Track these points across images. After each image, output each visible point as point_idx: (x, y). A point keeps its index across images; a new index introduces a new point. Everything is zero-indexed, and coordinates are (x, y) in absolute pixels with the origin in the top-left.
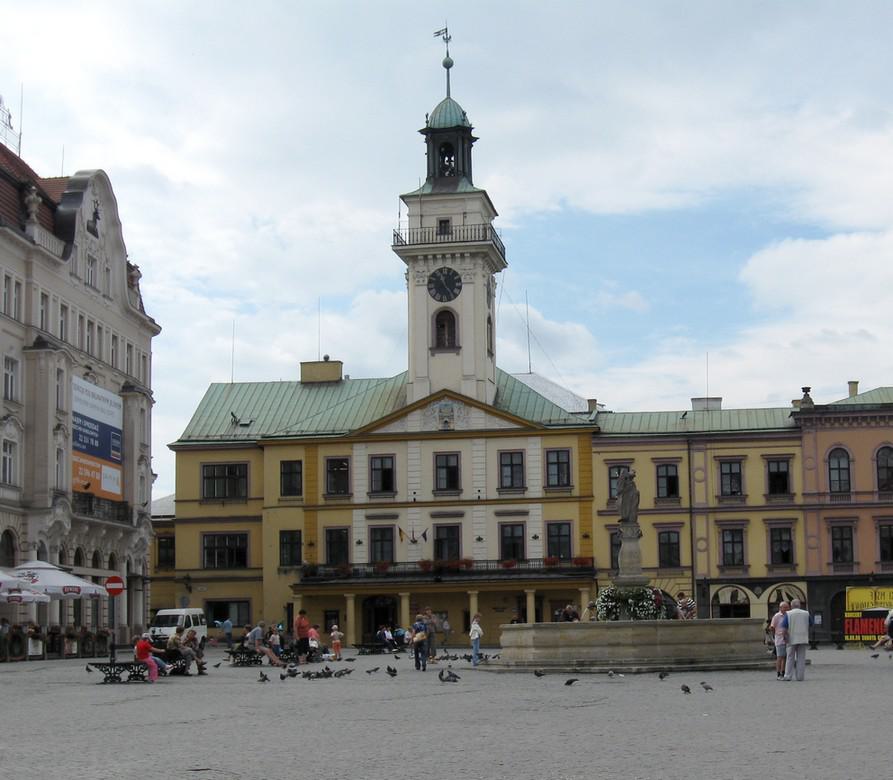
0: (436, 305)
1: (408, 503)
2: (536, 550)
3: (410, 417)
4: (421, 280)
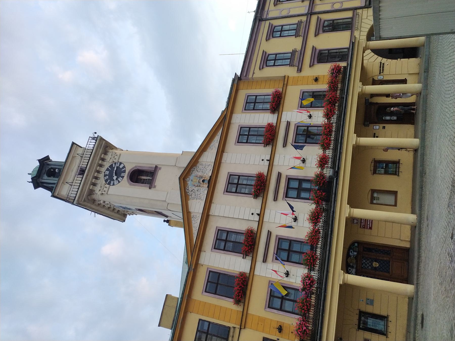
0: (125, 180)
1: (259, 221)
2: (318, 117)
3: (191, 209)
4: (105, 189)
